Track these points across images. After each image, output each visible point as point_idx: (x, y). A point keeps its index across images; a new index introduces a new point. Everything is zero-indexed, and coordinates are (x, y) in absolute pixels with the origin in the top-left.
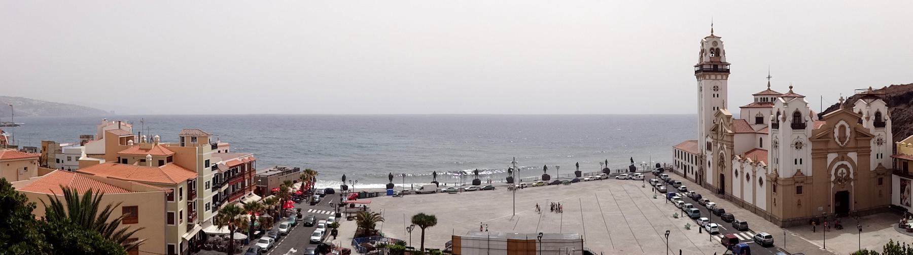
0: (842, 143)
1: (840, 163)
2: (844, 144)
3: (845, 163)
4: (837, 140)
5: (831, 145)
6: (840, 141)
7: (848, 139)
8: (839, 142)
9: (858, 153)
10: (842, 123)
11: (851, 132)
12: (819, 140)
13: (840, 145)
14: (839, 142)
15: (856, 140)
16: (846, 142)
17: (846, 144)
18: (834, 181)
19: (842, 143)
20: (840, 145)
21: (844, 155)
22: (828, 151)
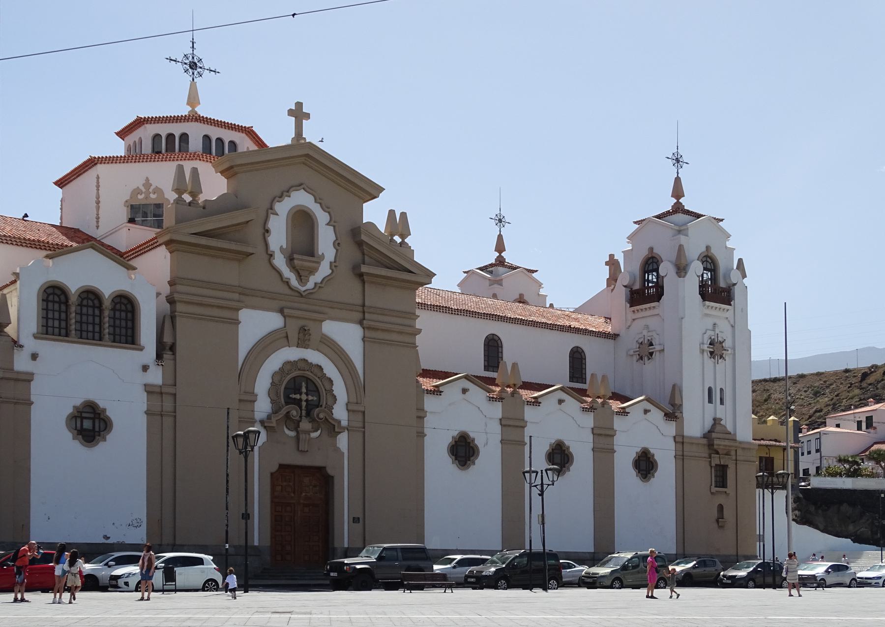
1: (292, 354)
2: (310, 285)
7: (324, 270)
8: (287, 273)
11: (337, 244)
12: (203, 241)
13: (294, 282)
14: (287, 273)
15: (361, 276)
18: (269, 417)
20: (294, 282)
21: (310, 325)
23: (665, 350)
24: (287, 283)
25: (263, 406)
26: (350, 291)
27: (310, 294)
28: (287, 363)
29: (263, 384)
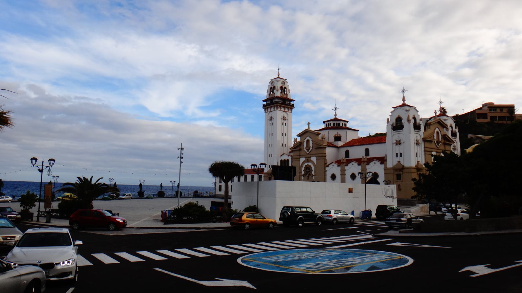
0: (308, 150)
1: (306, 164)
2: (309, 152)
3: (310, 164)
4: (305, 149)
5: (302, 153)
6: (306, 150)
7: (311, 149)
9: (316, 157)
10: (308, 138)
11: (313, 144)
13: (307, 152)
14: (306, 151)
15: (316, 148)
16: (310, 151)
17: (310, 152)
19: (308, 151)
20: (307, 152)
21: (309, 159)
22: (300, 156)
23: (391, 144)
24: (306, 152)
25: (303, 173)
26: (315, 152)
27: (308, 154)
28: (306, 165)
29: (303, 169)
